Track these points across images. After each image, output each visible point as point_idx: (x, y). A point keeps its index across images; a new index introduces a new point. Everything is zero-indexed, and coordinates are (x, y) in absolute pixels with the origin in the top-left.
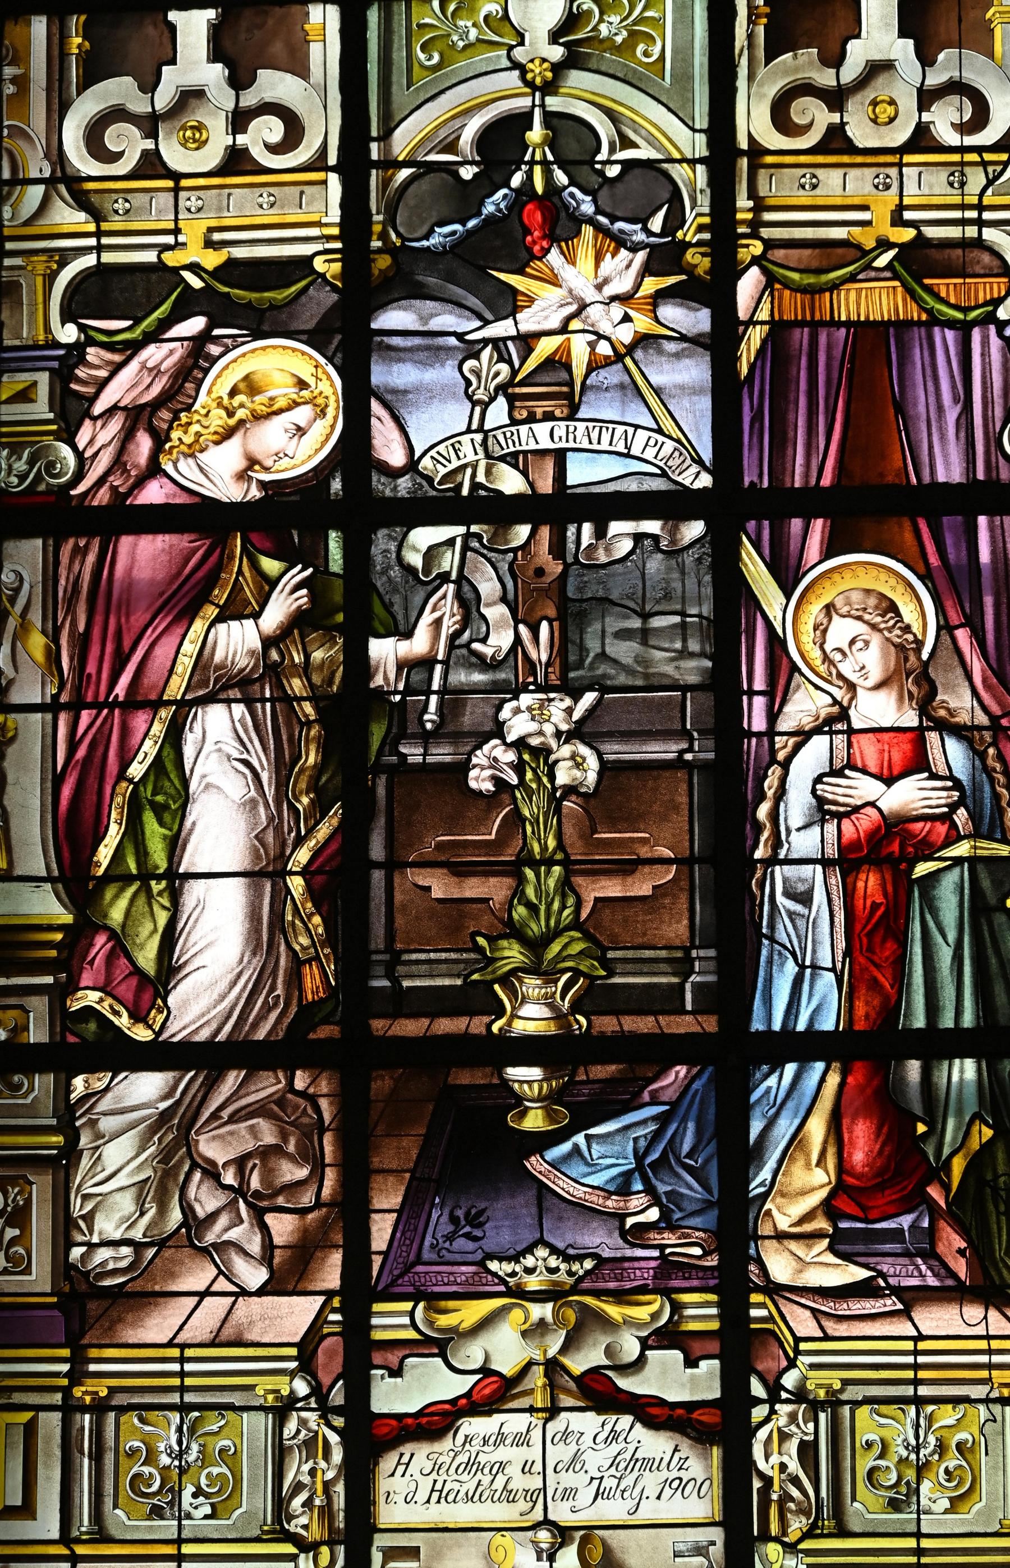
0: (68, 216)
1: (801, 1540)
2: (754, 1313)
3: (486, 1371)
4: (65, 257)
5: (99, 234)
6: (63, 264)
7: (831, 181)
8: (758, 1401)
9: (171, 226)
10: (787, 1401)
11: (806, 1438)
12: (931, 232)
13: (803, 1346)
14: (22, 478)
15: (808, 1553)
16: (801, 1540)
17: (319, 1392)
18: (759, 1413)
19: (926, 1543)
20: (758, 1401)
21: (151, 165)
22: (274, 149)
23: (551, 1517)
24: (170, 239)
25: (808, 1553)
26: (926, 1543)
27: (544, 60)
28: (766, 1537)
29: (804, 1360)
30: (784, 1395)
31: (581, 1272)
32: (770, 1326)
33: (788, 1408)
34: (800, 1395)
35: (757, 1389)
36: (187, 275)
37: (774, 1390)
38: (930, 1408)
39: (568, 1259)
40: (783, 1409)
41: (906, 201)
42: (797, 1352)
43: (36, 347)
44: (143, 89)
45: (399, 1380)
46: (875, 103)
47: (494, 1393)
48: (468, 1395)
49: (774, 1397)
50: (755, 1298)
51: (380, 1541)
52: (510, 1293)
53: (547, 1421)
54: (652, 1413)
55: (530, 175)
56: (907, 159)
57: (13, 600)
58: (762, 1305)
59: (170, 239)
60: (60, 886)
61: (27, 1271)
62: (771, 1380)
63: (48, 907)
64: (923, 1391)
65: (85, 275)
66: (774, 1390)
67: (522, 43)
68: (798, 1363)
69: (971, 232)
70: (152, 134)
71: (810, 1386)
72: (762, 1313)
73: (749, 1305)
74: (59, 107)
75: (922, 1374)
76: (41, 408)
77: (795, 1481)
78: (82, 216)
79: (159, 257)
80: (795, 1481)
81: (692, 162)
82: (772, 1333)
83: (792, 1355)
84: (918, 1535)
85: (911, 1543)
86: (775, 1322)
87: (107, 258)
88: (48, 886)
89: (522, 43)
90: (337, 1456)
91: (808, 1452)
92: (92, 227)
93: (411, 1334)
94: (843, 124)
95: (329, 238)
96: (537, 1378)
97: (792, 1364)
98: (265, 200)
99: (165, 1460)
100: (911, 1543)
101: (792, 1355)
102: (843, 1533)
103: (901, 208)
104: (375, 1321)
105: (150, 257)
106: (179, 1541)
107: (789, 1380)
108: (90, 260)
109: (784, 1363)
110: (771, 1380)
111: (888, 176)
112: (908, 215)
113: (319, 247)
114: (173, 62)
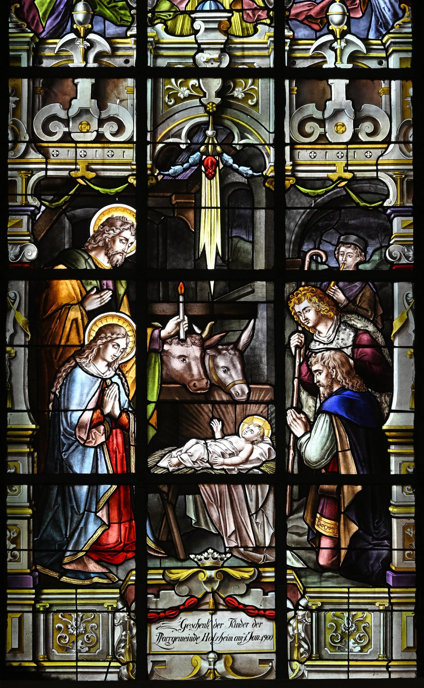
0: (34, 156)
3: (190, 596)
4: (32, 172)
5: (47, 163)
6: (32, 175)
7: (320, 154)
8: (290, 610)
9: (74, 161)
10: (301, 610)
12: (359, 174)
16: (305, 661)
18: (290, 614)
19: (351, 663)
20: (290, 610)
21: (66, 138)
22: (114, 135)
23: (214, 650)
24: (73, 167)
26: (351, 663)
27: (213, 103)
28: (293, 660)
30: (300, 608)
32: (295, 582)
34: (306, 608)
35: (289, 605)
36: (80, 181)
38: (354, 613)
40: (300, 613)
41: (349, 162)
42: (305, 592)
43: (21, 206)
44: (64, 109)
45: (158, 599)
46: (337, 125)
47: (194, 605)
50: (289, 571)
51: (150, 659)
52: (199, 567)
53: (212, 614)
54: (253, 612)
55: (207, 148)
56: (350, 146)
57: (13, 304)
59: (73, 167)
64: (351, 607)
65: (40, 180)
67: (205, 96)
69: (374, 174)
70: (68, 126)
71: (310, 604)
72: (292, 577)
73: (286, 574)
74: (32, 113)
75: (351, 601)
78: (40, 156)
79: (69, 173)
80: (304, 640)
81: (269, 145)
84: (349, 660)
85: (346, 663)
86: (296, 581)
87: (50, 173)
89: (205, 96)
91: (308, 629)
92: (44, 160)
93: (163, 582)
94: (325, 133)
95: (133, 170)
96: (210, 599)
98: (110, 153)
100: (346, 663)
102: (321, 659)
103: (347, 165)
104: (149, 577)
105: (66, 173)
107: (303, 602)
108: (43, 173)
109: (300, 597)
110: (295, 603)
111: (342, 153)
112: (350, 168)
113: (130, 173)
114: (76, 98)
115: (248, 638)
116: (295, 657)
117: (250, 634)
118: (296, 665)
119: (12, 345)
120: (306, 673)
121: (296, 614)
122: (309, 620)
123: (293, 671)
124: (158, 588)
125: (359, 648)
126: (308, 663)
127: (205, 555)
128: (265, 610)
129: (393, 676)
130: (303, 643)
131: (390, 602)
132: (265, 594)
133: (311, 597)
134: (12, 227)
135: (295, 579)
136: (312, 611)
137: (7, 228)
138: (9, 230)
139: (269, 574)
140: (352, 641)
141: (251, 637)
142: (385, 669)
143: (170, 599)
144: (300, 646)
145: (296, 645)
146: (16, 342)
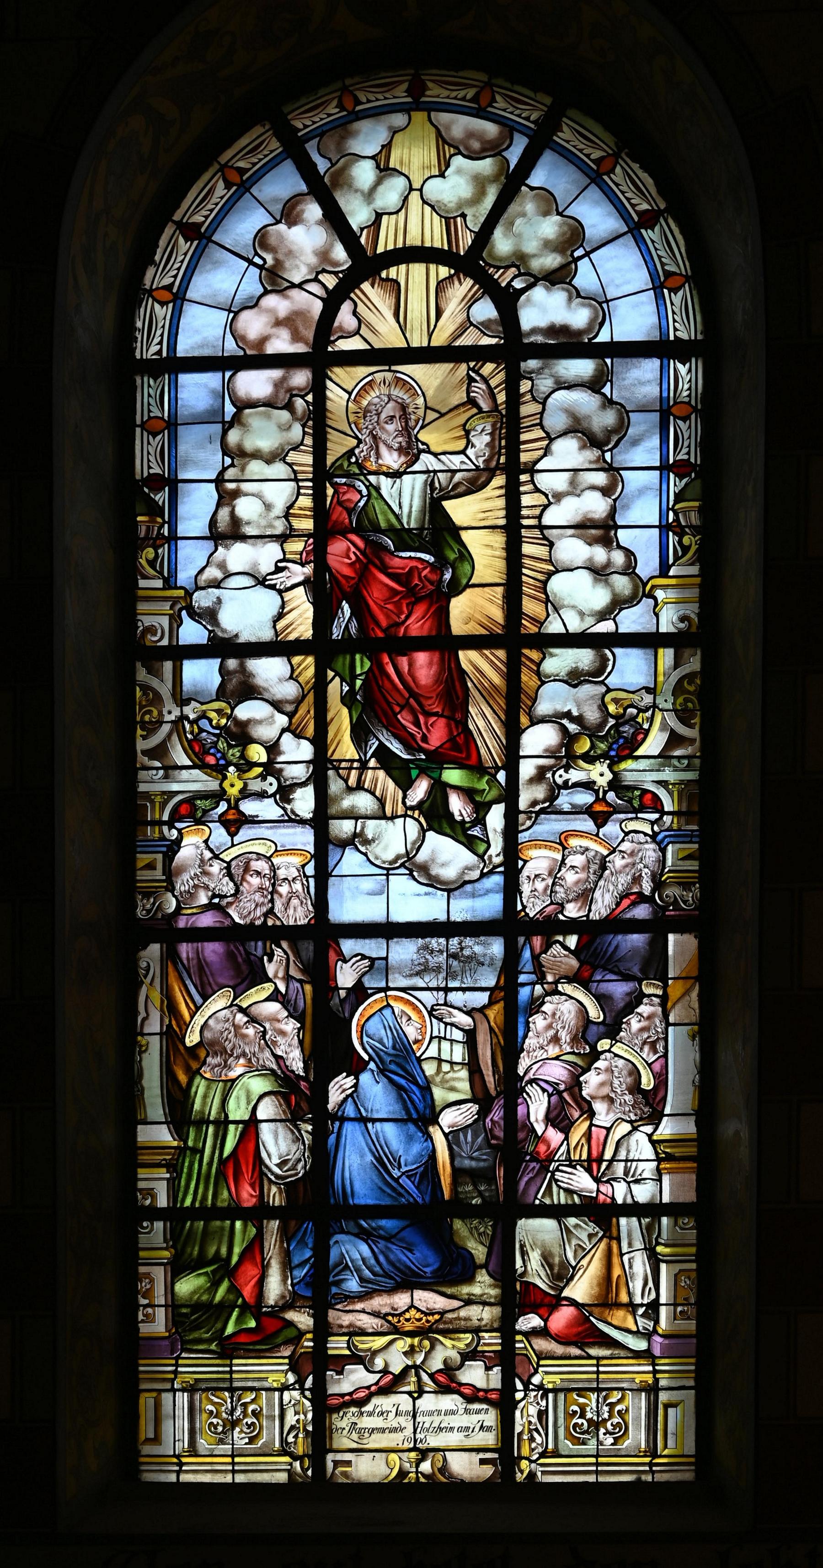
1: (538, 1459)
2: (517, 1345)
3: (385, 1371)
13: (542, 1362)
14: (149, 911)
15: (542, 1465)
16: (538, 1459)
17: (301, 1381)
25: (542, 1465)
29: (541, 1369)
30: (531, 1387)
33: (533, 1394)
34: (540, 1387)
35: (519, 1385)
37: (527, 1384)
38: (604, 1393)
39: (426, 1314)
42: (539, 1365)
48: (377, 1383)
49: (526, 1389)
51: (330, 1457)
58: (522, 1341)
61: (153, 1321)
63: (163, 1135)
66: (527, 1384)
72: (522, 1345)
76: (158, 874)
77: (537, 1430)
80: (537, 1430)
82: (526, 1355)
88: (165, 1126)
90: (310, 1416)
91: (542, 1415)
99: (224, 1415)
106: (233, 1456)
110: (525, 1378)
115: (477, 1429)
116: (525, 1452)
118: (524, 1464)
119: (143, 1035)
120: (539, 1474)
121: (526, 1395)
122: (544, 1403)
123: (522, 1472)
124: (340, 1363)
125: (612, 1441)
126: (542, 1461)
127: (407, 1316)
128: (486, 1391)
129: (658, 1477)
130: (535, 1435)
131: (654, 1377)
132: (488, 1369)
133: (547, 1373)
134: (142, 869)
135: (525, 1348)
136: (546, 1392)
137: (133, 870)
138: (139, 873)
139: (491, 1341)
140: (602, 1431)
141: (482, 1427)
142: (647, 1468)
143: (357, 1377)
144: (532, 1439)
145: (525, 1437)
146: (146, 1030)
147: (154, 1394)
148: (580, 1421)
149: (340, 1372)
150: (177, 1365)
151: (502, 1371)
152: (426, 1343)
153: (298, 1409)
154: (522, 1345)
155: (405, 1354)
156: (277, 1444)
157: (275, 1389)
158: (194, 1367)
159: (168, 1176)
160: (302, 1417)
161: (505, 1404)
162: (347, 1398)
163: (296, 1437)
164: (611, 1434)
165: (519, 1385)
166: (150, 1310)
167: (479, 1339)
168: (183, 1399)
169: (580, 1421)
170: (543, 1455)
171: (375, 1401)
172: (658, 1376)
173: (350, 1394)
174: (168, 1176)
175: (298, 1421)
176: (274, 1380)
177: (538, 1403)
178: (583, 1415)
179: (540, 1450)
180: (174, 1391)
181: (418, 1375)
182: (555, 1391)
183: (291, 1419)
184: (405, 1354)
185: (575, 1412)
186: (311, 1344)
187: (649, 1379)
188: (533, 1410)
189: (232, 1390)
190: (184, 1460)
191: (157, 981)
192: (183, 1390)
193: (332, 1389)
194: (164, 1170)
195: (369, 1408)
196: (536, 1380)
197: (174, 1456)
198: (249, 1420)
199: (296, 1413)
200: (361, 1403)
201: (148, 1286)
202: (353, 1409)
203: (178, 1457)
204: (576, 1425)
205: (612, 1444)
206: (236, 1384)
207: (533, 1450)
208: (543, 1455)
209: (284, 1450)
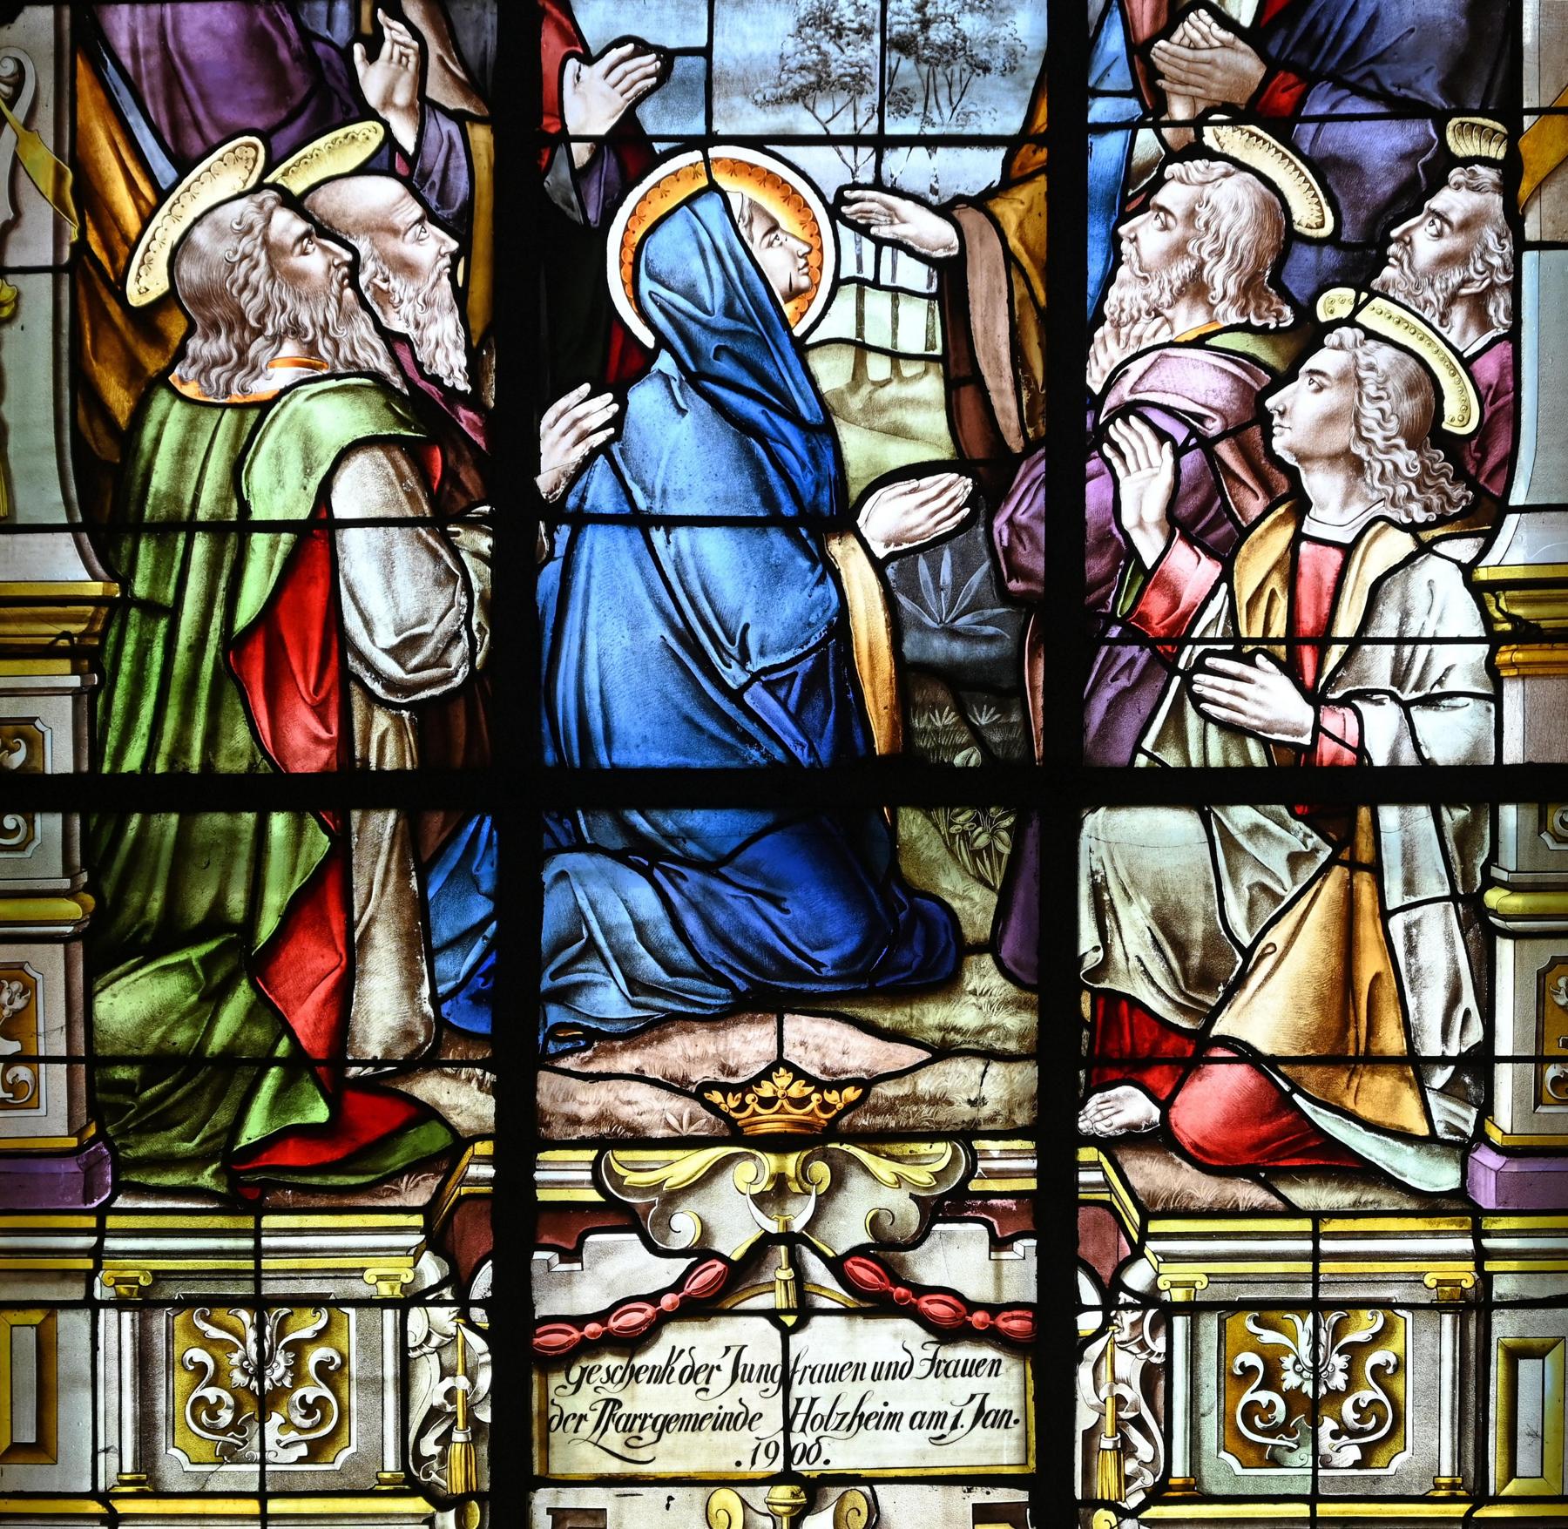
1: (1143, 1506)
10: (1127, 1307)
11: (1154, 1360)
13: (1155, 1226)
16: (1143, 1506)
30: (1124, 1297)
31: (840, 1106)
32: (1106, 1197)
33: (1128, 1317)
34: (1149, 1299)
37: (1110, 1290)
38: (1334, 1317)
39: (820, 1086)
42: (1145, 1236)
45: (577, 1266)
50: (1087, 1154)
58: (1096, 1165)
60: (85, 537)
61: (33, 1103)
62: (1106, 1273)
63: (63, 564)
68: (1146, 1251)
72: (1096, 1177)
73: (1076, 1166)
77: (1139, 1423)
80: (1139, 1423)
82: (1108, 1205)
83: (1135, 1237)
86: (1112, 1191)
88: (67, 538)
90: (485, 1379)
91: (1155, 1377)
97: (1138, 1253)
99: (238, 1378)
101: (1135, 1237)
110: (1106, 1273)
115: (967, 1420)
116: (1106, 1484)
117: (978, 1400)
122: (1160, 1345)
125: (1354, 1454)
127: (766, 1090)
128: (994, 1309)
130: (1135, 1436)
132: (998, 1244)
133: (1168, 1258)
135: (1107, 1183)
136: (1167, 1312)
140: (1329, 1425)
141: (981, 1414)
143: (617, 1270)
144: (1125, 1449)
145: (1107, 1443)
147: (37, 1317)
148: (1264, 1397)
149: (572, 1255)
150: (101, 1232)
151: (1039, 1251)
152: (821, 1170)
153: (452, 1362)
154: (1096, 1177)
155: (760, 1200)
156: (391, 1462)
157: (385, 1303)
158: (154, 1237)
159: (75, 681)
160: (462, 1383)
161: (1046, 1344)
162: (592, 1327)
163: (445, 1440)
164: (1353, 1434)
165: (1088, 1293)
166: (23, 1073)
167: (974, 1157)
168: (118, 1329)
169: (1264, 1397)
170: (1157, 1495)
171: (675, 1336)
172: (1489, 1266)
173: (601, 1317)
174: (75, 681)
175: (450, 1395)
176: (384, 1274)
177: (1143, 1346)
178: (1271, 1380)
179: (1149, 1480)
180: (92, 1305)
181: (795, 1263)
182: (1193, 1309)
183: (429, 1390)
184: (760, 1200)
185: (1249, 1371)
186: (488, 1171)
187: (1465, 1274)
188: (1129, 1366)
189: (259, 1304)
190: (122, 1507)
191: (46, 115)
192: (120, 1304)
193: (549, 1303)
194: (66, 665)
195: (654, 1356)
196: (1137, 1277)
197: (94, 1495)
198: (311, 1392)
199: (446, 1372)
200: (633, 1342)
201: (19, 1003)
202: (610, 1361)
203: (105, 1497)
204: (1251, 1408)
205: (1357, 1465)
206: (271, 1288)
207: (1129, 1480)
208: (1157, 1495)
209: (410, 1479)
